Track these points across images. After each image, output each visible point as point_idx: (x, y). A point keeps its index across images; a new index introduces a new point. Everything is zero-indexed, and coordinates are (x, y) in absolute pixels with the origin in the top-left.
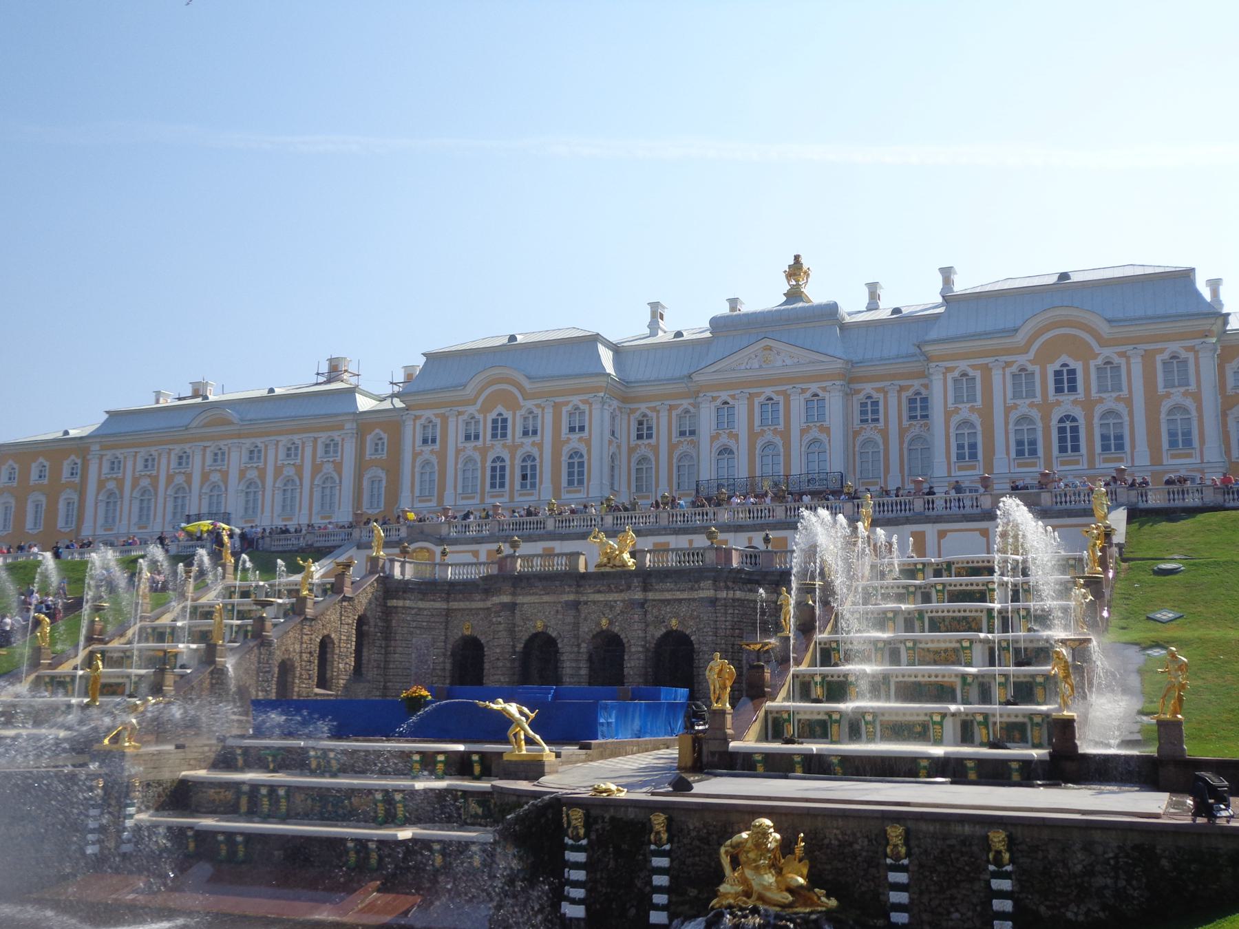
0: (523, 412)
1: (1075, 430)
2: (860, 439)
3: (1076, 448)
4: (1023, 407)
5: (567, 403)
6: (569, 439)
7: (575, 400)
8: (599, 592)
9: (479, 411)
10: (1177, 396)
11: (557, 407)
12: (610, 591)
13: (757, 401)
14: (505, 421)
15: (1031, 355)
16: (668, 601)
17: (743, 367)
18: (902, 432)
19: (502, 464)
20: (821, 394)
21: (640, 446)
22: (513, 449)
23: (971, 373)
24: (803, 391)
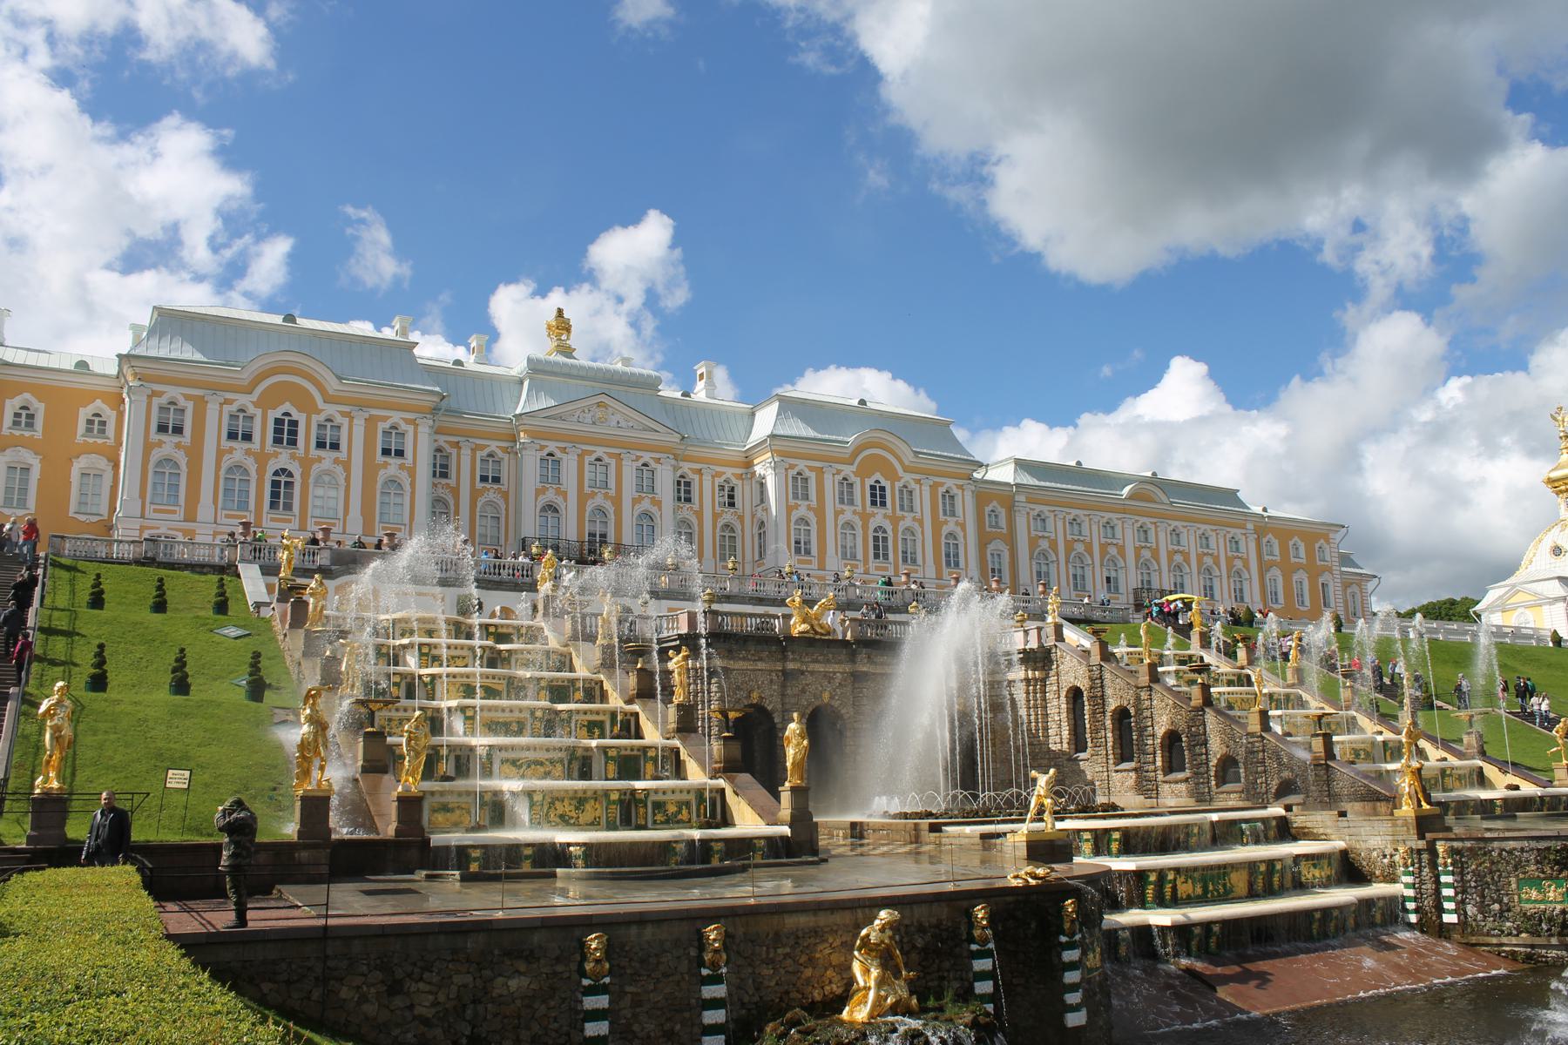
0: (322, 417)
1: (885, 539)
3: (886, 556)
4: (848, 514)
5: (385, 419)
7: (396, 417)
8: (816, 661)
9: (256, 404)
10: (950, 526)
11: (371, 422)
12: (828, 661)
13: (588, 459)
14: (294, 423)
15: (854, 468)
17: (575, 418)
18: (716, 516)
20: (653, 465)
22: (306, 464)
23: (807, 473)
24: (638, 458)
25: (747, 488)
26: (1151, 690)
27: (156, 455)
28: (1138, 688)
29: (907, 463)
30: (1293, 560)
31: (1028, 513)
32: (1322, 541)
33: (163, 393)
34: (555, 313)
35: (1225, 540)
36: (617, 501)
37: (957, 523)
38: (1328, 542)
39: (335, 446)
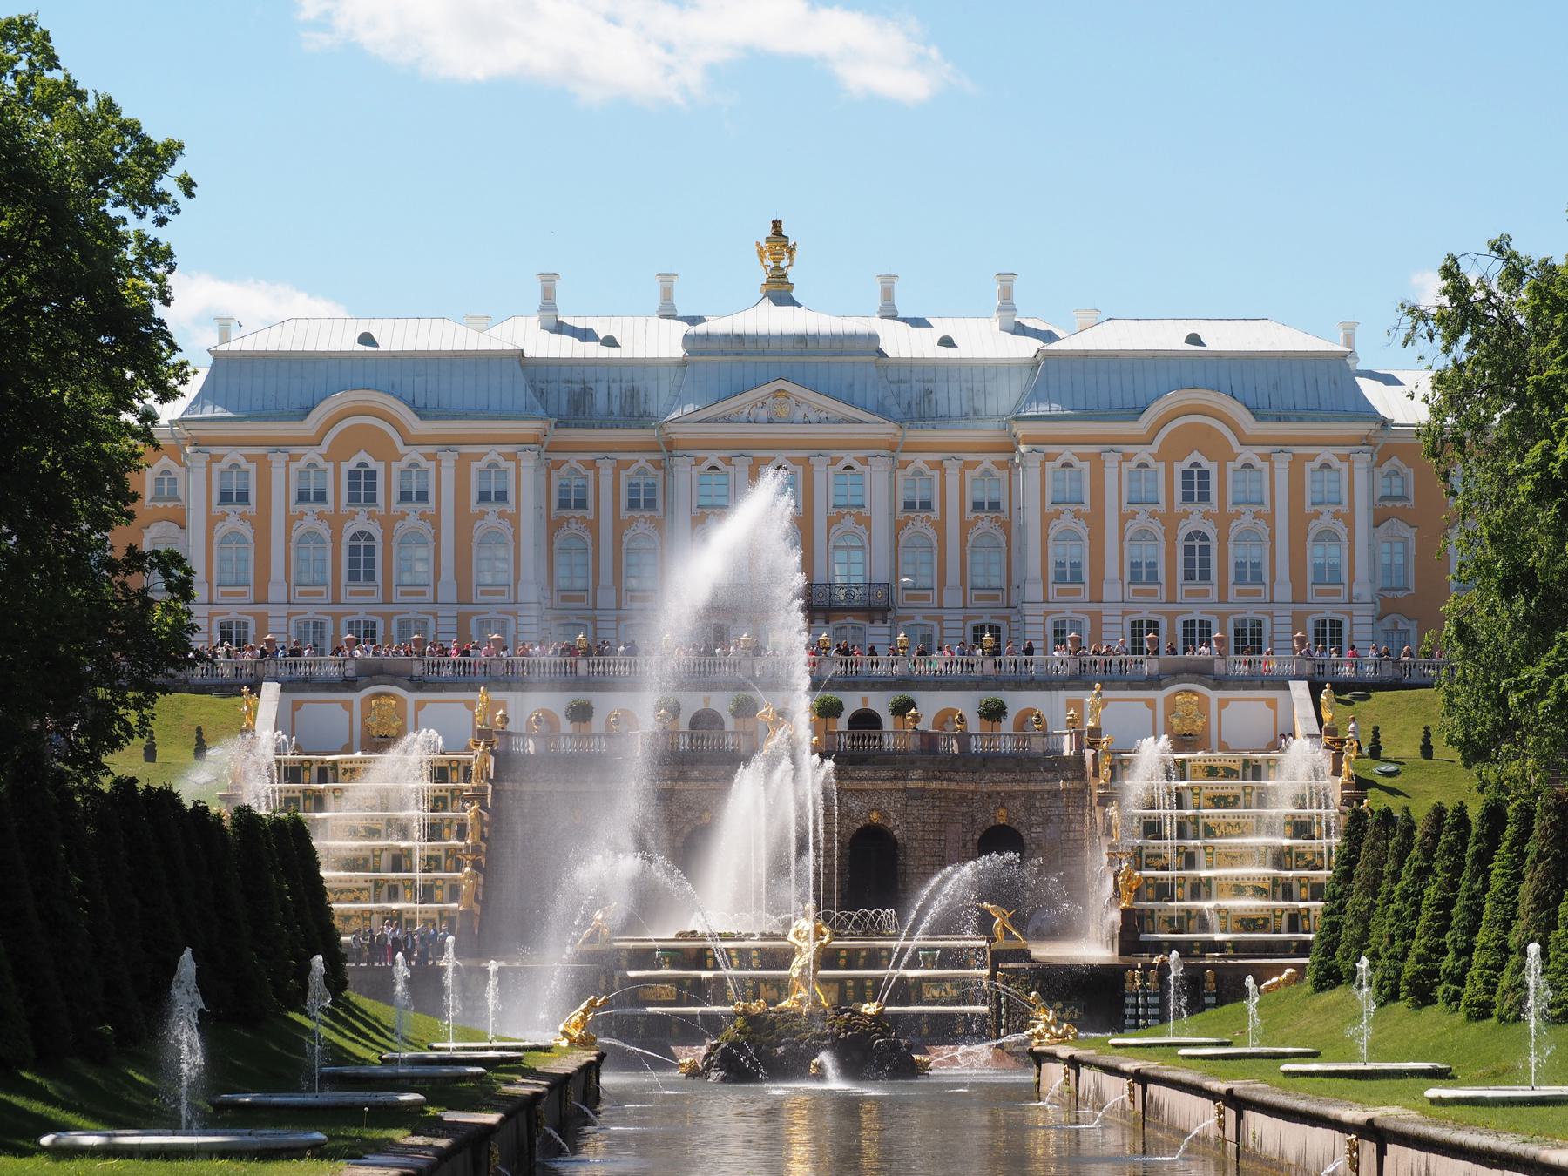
1: (1205, 550)
2: (905, 534)
3: (1205, 576)
4: (1142, 520)
5: (479, 457)
6: (483, 515)
7: (493, 453)
9: (326, 458)
10: (1326, 521)
11: (463, 464)
14: (372, 475)
15: (1154, 448)
16: (866, 791)
18: (965, 527)
19: (368, 543)
21: (568, 520)
22: (388, 523)
27: (221, 530)
29: (1248, 432)
33: (223, 456)
34: (769, 232)
39: (422, 497)
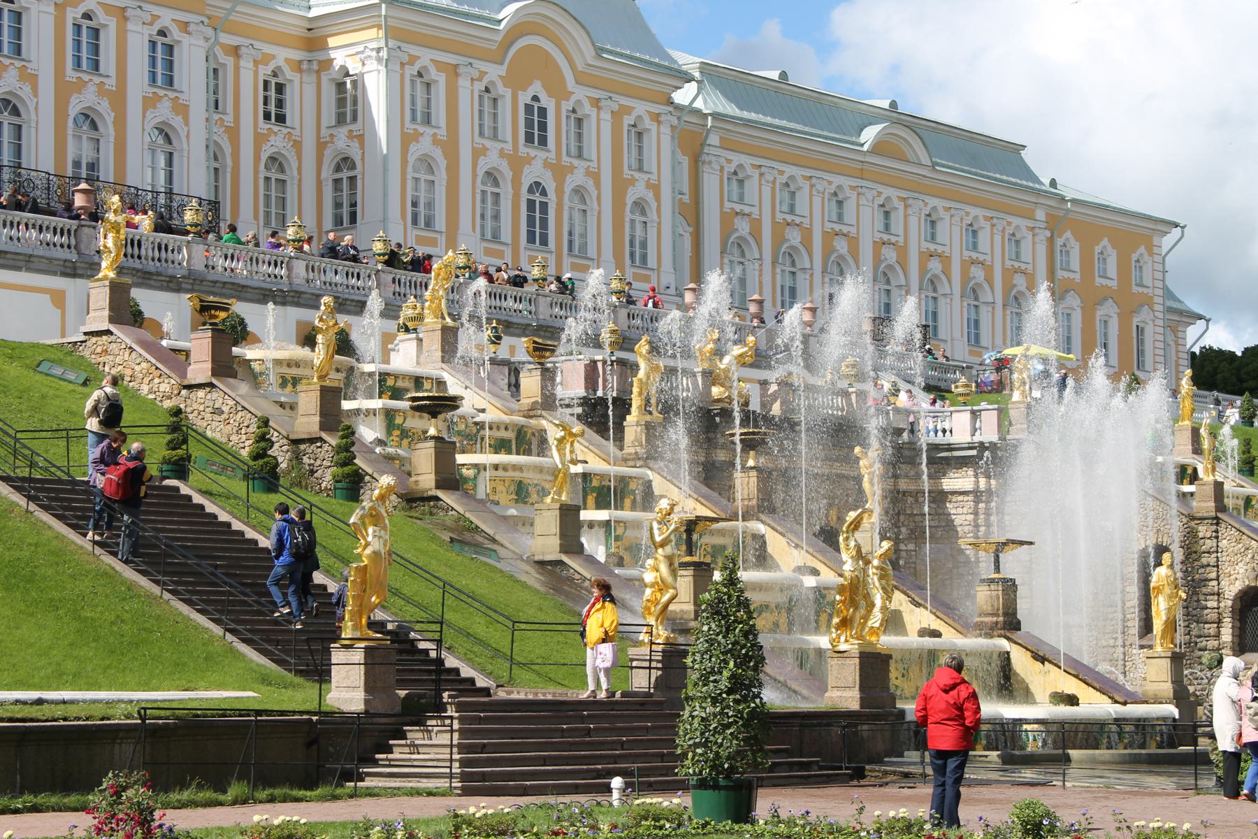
1: (544, 206)
3: (544, 242)
15: (502, 70)
18: (260, 139)
20: (176, 33)
23: (434, 74)
25: (310, 91)
26: (1217, 524)
28: (1192, 518)
30: (1099, 281)
31: (722, 168)
32: (1142, 249)
35: (1003, 238)
36: (118, 99)
37: (649, 185)
38: (1151, 254)
